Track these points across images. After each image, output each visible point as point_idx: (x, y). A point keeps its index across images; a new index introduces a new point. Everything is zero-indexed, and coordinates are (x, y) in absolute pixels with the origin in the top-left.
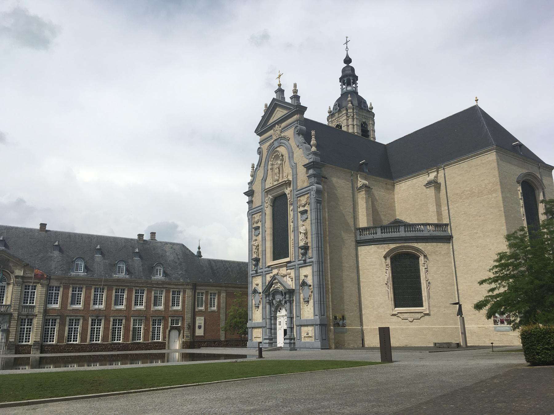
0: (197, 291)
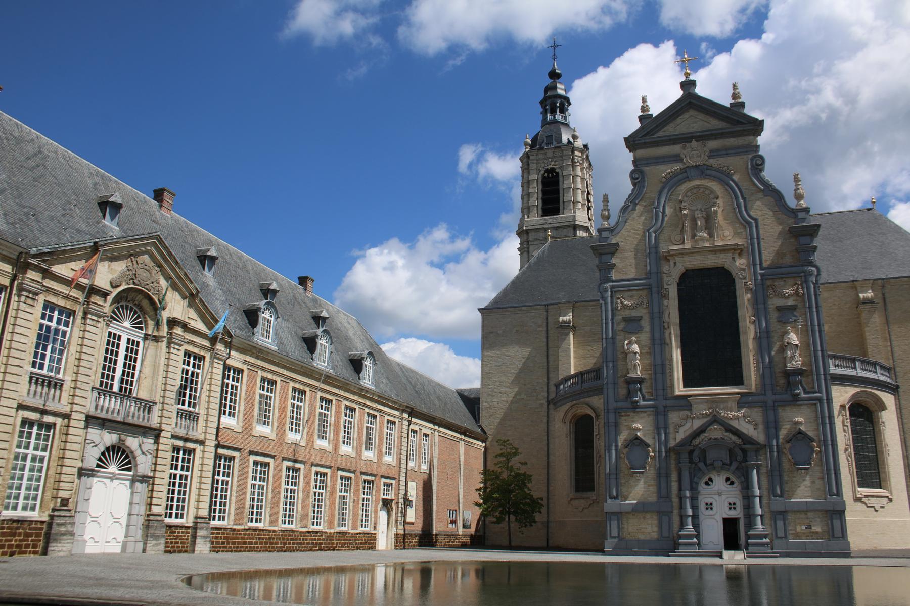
0: (412, 427)
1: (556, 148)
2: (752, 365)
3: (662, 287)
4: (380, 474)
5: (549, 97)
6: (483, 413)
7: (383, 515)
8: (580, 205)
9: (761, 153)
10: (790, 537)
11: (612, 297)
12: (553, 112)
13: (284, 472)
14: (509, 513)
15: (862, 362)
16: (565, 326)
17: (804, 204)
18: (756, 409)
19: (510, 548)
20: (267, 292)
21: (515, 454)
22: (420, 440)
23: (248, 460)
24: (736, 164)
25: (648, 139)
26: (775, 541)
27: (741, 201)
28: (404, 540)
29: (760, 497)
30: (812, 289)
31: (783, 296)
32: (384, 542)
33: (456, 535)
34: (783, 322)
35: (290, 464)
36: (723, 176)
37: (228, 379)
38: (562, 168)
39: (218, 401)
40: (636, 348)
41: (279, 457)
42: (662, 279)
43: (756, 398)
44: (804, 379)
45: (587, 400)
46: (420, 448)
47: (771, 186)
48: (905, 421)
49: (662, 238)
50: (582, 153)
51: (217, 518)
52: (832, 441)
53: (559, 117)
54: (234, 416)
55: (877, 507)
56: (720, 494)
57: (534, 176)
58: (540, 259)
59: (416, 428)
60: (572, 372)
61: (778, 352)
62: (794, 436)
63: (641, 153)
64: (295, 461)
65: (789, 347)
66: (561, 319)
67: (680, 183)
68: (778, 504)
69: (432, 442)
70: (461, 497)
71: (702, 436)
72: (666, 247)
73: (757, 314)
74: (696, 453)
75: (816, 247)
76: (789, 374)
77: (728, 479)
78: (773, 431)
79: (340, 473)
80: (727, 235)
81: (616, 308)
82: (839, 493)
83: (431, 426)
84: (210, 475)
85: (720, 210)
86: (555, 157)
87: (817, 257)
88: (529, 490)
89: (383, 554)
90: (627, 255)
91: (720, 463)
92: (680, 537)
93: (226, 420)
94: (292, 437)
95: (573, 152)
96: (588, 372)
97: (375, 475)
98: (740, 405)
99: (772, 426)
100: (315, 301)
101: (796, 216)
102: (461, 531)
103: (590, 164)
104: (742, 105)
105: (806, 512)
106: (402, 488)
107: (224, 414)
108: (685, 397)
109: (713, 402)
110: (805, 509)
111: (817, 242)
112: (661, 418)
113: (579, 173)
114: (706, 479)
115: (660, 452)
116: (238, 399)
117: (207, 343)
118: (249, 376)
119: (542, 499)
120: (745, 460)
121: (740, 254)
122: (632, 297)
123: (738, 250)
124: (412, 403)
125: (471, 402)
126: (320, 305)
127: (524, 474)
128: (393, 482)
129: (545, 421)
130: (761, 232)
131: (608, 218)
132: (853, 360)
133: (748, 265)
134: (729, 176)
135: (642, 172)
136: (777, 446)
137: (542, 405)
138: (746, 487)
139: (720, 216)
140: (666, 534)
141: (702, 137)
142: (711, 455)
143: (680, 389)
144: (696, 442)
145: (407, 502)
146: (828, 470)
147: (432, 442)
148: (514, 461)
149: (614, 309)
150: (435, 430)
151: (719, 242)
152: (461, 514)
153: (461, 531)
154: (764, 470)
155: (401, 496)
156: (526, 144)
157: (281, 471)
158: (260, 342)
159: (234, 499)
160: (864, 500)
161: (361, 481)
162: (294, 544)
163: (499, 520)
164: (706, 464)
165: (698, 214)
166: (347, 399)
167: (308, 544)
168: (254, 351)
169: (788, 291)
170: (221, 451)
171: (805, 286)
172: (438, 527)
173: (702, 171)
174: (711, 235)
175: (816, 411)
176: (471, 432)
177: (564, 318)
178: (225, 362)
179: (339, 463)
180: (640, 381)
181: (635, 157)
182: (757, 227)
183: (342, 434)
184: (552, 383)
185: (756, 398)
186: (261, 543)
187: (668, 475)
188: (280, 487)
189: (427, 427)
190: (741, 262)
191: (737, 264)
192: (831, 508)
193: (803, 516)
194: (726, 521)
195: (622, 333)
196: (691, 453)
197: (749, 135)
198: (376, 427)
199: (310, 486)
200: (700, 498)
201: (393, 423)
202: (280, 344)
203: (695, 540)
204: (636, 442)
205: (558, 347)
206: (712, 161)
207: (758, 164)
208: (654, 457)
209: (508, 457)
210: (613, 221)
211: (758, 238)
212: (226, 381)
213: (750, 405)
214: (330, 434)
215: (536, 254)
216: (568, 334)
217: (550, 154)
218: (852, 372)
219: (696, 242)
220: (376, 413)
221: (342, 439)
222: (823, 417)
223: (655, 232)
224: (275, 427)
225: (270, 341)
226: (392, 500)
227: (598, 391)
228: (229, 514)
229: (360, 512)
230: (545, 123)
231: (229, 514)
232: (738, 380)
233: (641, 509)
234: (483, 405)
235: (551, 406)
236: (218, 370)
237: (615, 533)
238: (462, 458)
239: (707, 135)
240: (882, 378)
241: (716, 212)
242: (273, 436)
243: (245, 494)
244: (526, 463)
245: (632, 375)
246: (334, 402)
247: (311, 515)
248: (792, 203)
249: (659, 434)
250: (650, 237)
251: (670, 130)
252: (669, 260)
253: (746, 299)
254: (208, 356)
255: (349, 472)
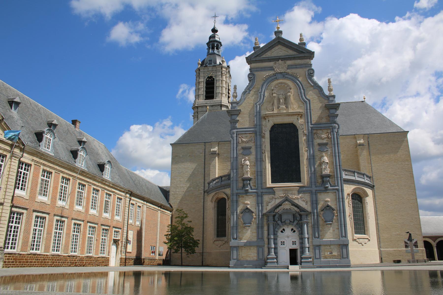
0: (131, 202)
1: (213, 66)
2: (305, 172)
3: (262, 132)
4: (112, 226)
5: (211, 41)
6: (171, 197)
7: (114, 248)
8: (224, 95)
9: (313, 67)
10: (322, 258)
11: (236, 137)
12: (213, 48)
13: (55, 223)
14: (181, 247)
15: (358, 173)
16: (214, 153)
17: (332, 93)
18: (307, 194)
19: (182, 265)
20: (51, 125)
21: (186, 217)
22: (136, 209)
23: (32, 215)
24: (300, 73)
25: (258, 58)
26: (315, 260)
27: (302, 91)
28: (125, 261)
29: (308, 238)
30: (336, 135)
31: (322, 138)
32: (114, 262)
33: (155, 260)
34: (321, 151)
35: (59, 218)
36: (294, 78)
37: (22, 169)
38: (216, 76)
39: (14, 181)
40: (248, 163)
41: (52, 214)
42: (262, 128)
43: (307, 189)
44: (330, 180)
45: (223, 190)
46: (136, 213)
47: (317, 84)
48: (377, 202)
49: (263, 108)
50: (226, 69)
51: (10, 248)
52: (343, 210)
53: (216, 51)
54: (24, 190)
55: (363, 244)
56: (288, 237)
57: (202, 80)
58: (203, 120)
59: (134, 202)
60: (217, 176)
61: (318, 166)
62: (325, 208)
63: (254, 65)
64: (62, 217)
65: (323, 163)
66: (212, 150)
67: (273, 81)
68: (317, 242)
69: (142, 210)
70: (158, 239)
71: (280, 208)
72: (264, 112)
73: (308, 147)
74: (277, 216)
75: (338, 115)
76: (323, 177)
77: (292, 229)
78: (315, 205)
79: (89, 224)
80: (295, 107)
81: (239, 143)
82: (346, 236)
83: (142, 202)
84: (6, 222)
85: (292, 95)
86: (213, 71)
87: (338, 120)
88: (192, 235)
89: (113, 269)
90: (245, 116)
91: (289, 221)
92: (268, 259)
93: (18, 192)
94: (60, 203)
95: (222, 68)
96: (225, 176)
97: (109, 226)
98: (299, 192)
99: (315, 203)
100: (81, 133)
101: (329, 99)
102: (157, 257)
103: (230, 76)
104: (304, 44)
105: (330, 245)
106: (125, 234)
107: (18, 188)
108: (272, 188)
109: (286, 190)
110: (329, 244)
111: (338, 112)
112: (260, 198)
113: (225, 79)
114: (281, 229)
115: (259, 215)
116: (27, 180)
117: (8, 148)
118: (35, 168)
119: (199, 240)
120: (301, 220)
121: (301, 117)
122: (247, 137)
123: (300, 115)
124: (132, 189)
125: (165, 192)
126: (84, 136)
127: (190, 228)
128: (120, 230)
129: (202, 201)
130: (312, 106)
131: (236, 97)
132: (354, 172)
133: (305, 122)
134: (297, 78)
135: (254, 75)
136: (317, 213)
137: (201, 193)
138: (301, 233)
139: (292, 98)
140: (261, 257)
141: (284, 59)
142: (284, 217)
143: (269, 184)
144: (277, 210)
145: (127, 241)
146: (341, 225)
147: (142, 210)
148: (185, 221)
149: (237, 143)
150: (144, 204)
151: (291, 111)
152: (158, 248)
153: (157, 257)
154: (310, 225)
155: (124, 238)
156: (199, 64)
157: (53, 222)
158: (43, 150)
159: (21, 237)
160: (357, 240)
161: (101, 229)
162: (59, 262)
163: (176, 251)
164: (281, 222)
165: (281, 96)
166: (95, 185)
167: (68, 262)
168: (39, 155)
169: (324, 136)
170: (14, 209)
171: (332, 133)
172: (145, 255)
173: (284, 75)
174: (287, 107)
175: (336, 195)
176: (164, 206)
177: (214, 149)
178: (20, 160)
179: (88, 219)
180: (250, 179)
181: (250, 67)
182: (310, 104)
183: (91, 203)
184: (206, 182)
185: (307, 189)
186: (38, 262)
187: (262, 227)
188: (52, 231)
189: (140, 202)
190: (301, 121)
191: (299, 121)
192: (342, 243)
193: (328, 247)
194: (290, 249)
195: (241, 155)
196: (274, 216)
197: (307, 59)
198: (111, 201)
199: (70, 231)
200: (278, 239)
201: (121, 199)
202: (56, 152)
203: (275, 260)
204: (247, 210)
205: (210, 164)
206: (289, 71)
207: (311, 73)
208: (256, 218)
209: (182, 218)
210: (238, 99)
211: (310, 110)
212: (20, 170)
213: (304, 192)
214: (84, 202)
215: (201, 118)
216: (215, 158)
217: (210, 69)
218: (353, 178)
219: (280, 110)
220: (111, 193)
221: (90, 206)
222: (339, 198)
223: (259, 105)
224: (50, 198)
225: (50, 150)
226: (119, 240)
227: (228, 186)
228: (18, 245)
229: (100, 246)
230: (209, 54)
231: (18, 245)
232: (298, 180)
233: (249, 245)
234: (171, 193)
235: (206, 194)
236: (15, 163)
237: (235, 257)
238: (159, 219)
239: (286, 58)
240: (367, 181)
241: (290, 96)
242: (49, 203)
243: (29, 234)
244: (191, 222)
245: (246, 176)
246: (87, 186)
247: (70, 246)
248: (327, 93)
249: (258, 206)
250: (256, 107)
251: (269, 54)
252: (266, 119)
253: (303, 139)
254: (9, 155)
255: (93, 223)
